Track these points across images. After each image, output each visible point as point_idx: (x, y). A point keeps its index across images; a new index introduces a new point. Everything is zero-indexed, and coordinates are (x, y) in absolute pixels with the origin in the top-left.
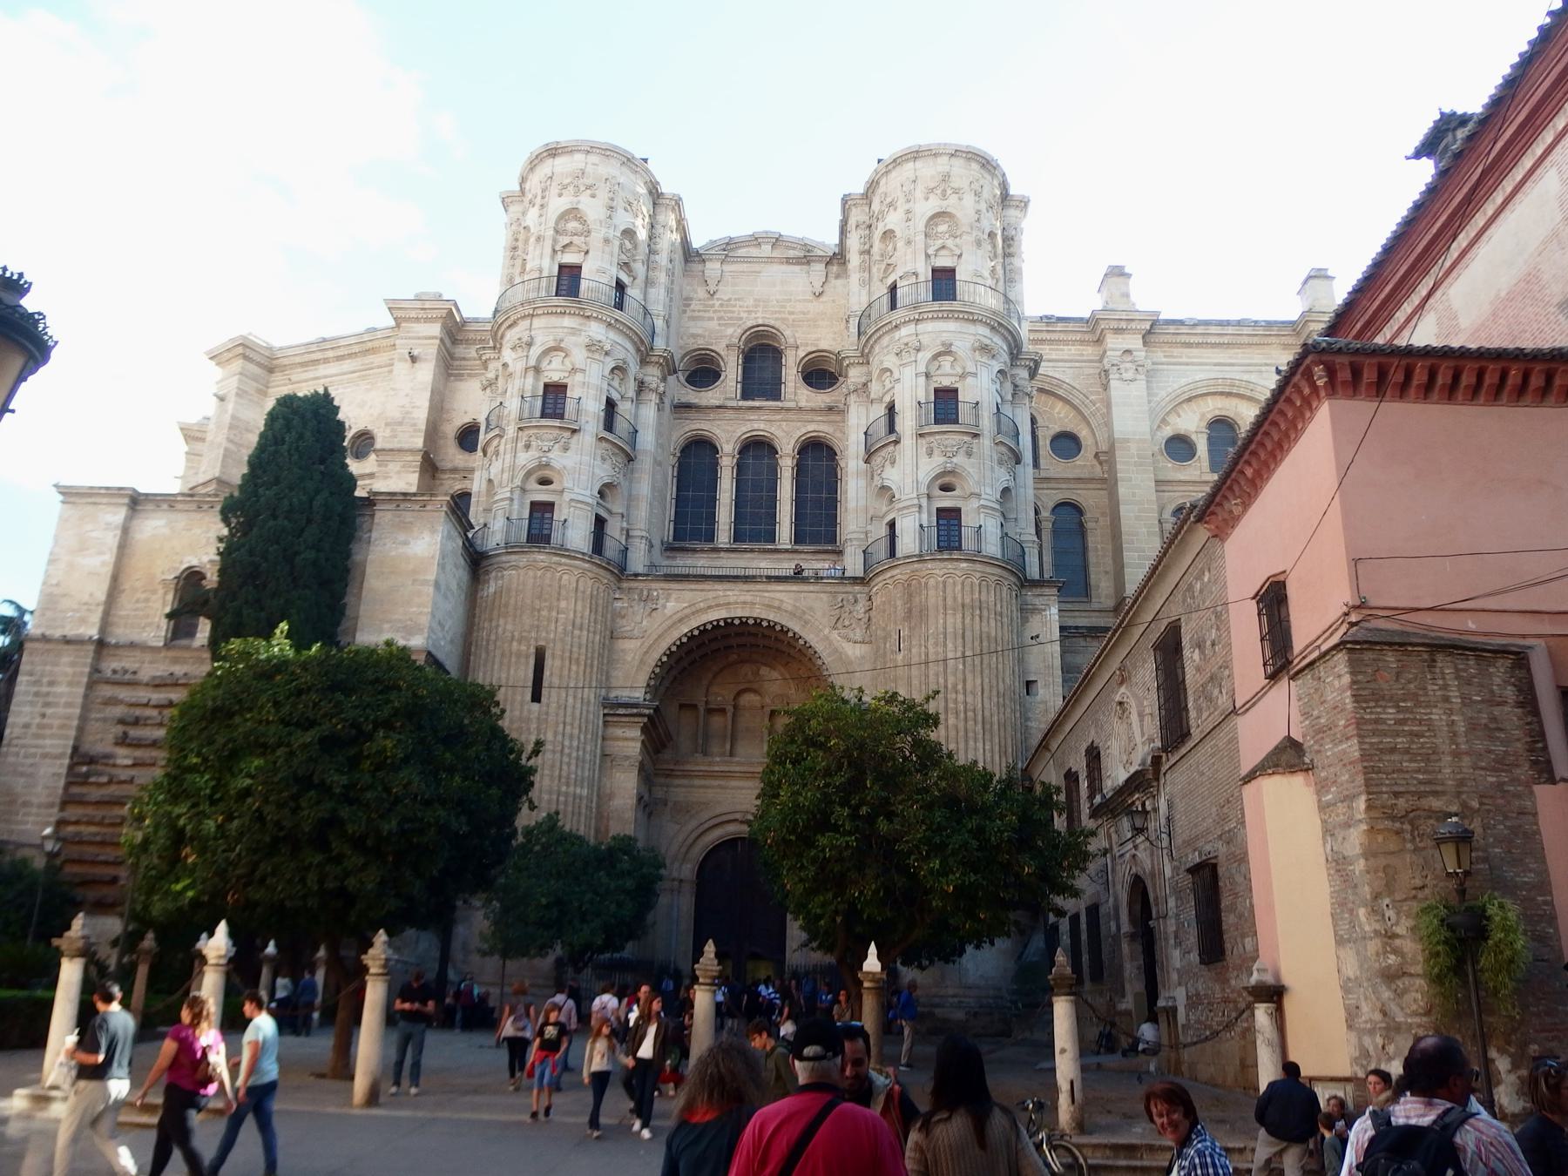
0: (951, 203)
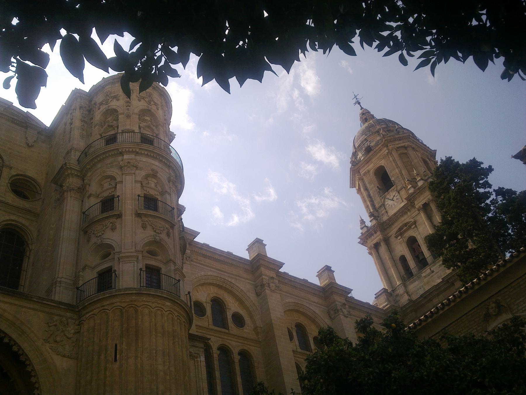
0: (154, 108)
